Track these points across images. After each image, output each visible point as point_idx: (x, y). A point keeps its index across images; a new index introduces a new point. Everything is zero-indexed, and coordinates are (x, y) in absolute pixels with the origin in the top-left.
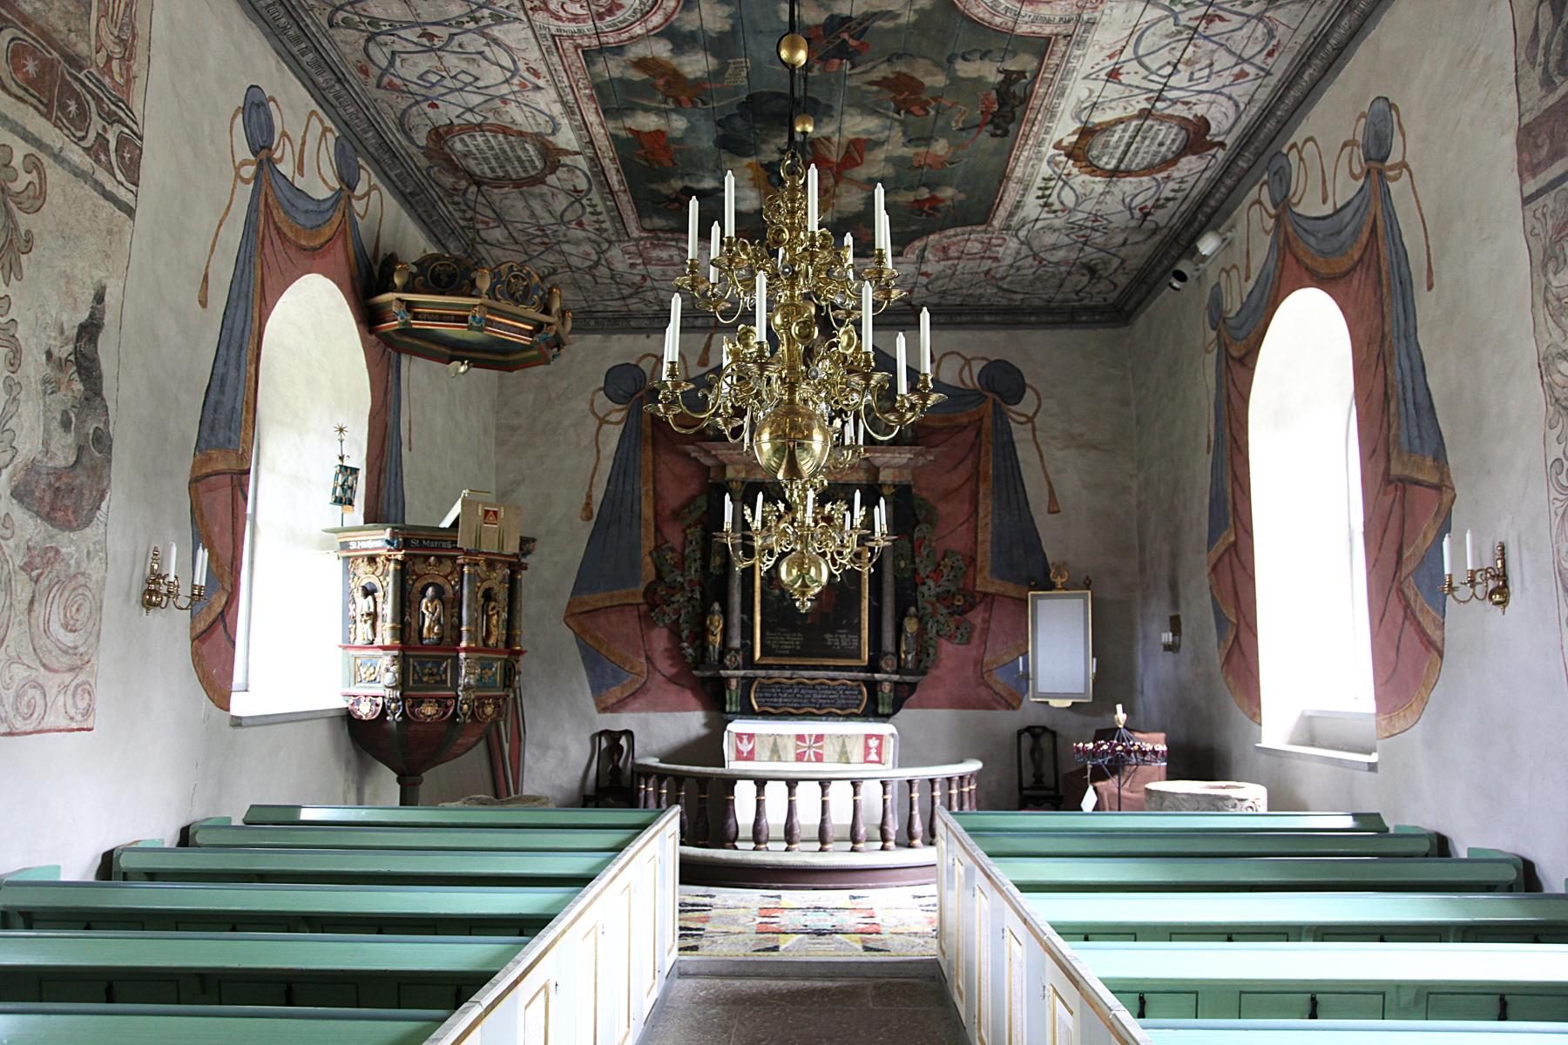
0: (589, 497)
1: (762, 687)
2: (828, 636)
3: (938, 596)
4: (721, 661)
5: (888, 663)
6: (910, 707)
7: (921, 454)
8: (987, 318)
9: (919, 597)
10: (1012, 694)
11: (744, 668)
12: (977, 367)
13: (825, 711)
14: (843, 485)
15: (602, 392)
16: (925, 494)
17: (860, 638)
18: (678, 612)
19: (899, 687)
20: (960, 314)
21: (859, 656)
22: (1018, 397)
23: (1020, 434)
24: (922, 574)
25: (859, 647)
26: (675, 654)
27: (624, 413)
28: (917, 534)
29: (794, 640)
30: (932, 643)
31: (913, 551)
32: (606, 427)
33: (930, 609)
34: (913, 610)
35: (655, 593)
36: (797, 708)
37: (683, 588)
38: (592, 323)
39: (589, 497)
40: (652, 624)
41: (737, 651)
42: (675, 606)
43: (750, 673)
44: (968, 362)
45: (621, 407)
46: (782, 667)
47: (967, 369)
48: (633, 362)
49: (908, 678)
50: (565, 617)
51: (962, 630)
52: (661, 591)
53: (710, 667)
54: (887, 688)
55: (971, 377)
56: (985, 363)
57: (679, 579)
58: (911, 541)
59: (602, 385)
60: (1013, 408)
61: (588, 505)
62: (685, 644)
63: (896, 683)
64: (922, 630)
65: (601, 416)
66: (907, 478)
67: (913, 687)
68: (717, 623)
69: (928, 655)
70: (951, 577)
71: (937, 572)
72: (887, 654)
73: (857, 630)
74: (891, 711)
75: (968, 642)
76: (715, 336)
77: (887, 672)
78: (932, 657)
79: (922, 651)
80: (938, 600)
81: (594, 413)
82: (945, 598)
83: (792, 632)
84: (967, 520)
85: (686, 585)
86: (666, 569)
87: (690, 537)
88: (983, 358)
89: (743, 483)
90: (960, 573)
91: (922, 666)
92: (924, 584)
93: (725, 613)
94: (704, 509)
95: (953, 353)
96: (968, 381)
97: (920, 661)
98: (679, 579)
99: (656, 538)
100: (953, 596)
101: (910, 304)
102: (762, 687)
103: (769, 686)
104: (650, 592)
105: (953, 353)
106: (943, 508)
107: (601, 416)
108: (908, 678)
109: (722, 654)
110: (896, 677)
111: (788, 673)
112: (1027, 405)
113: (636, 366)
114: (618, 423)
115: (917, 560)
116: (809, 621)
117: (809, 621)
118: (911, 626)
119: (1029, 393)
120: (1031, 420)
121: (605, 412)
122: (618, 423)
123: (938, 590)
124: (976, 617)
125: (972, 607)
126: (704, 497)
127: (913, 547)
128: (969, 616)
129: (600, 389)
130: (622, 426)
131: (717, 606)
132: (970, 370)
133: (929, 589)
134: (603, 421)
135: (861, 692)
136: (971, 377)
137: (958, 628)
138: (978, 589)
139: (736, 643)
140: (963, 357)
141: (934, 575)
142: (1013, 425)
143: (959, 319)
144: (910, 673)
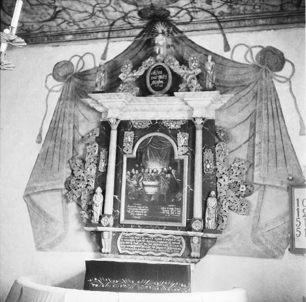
0: (41, 130)
1: (124, 238)
2: (163, 208)
3: (229, 186)
4: (100, 222)
5: (197, 225)
6: (212, 253)
7: (217, 100)
8: (261, 22)
9: (218, 186)
10: (277, 248)
11: (114, 226)
12: (256, 51)
13: (160, 254)
14: (174, 120)
15: (51, 77)
16: (223, 125)
17: (182, 210)
18: (80, 193)
19: (205, 241)
20: (244, 20)
21: (180, 221)
22: (280, 67)
23: (281, 89)
24: (221, 172)
25: (181, 216)
26: (80, 218)
27: (61, 86)
28: (217, 148)
29: (142, 210)
30: (224, 214)
31: (215, 158)
32: (52, 94)
33: (224, 193)
34: (213, 193)
35: (70, 183)
36: (143, 252)
37: (83, 180)
38: (46, 39)
39: (41, 130)
40: (68, 202)
41: (109, 216)
42: (80, 190)
43: (117, 229)
44: (250, 49)
45: (61, 83)
46: (136, 226)
47: (249, 54)
48: (68, 60)
49: (210, 235)
50: (24, 197)
51: (244, 206)
52: (73, 182)
53: (95, 225)
54: (195, 240)
55: (252, 57)
56: (260, 49)
57: (82, 174)
58: (214, 152)
59: (51, 72)
60: (277, 73)
61: (40, 135)
62: (83, 212)
63: (202, 238)
64: (219, 205)
65: (50, 87)
66: (211, 116)
67: (214, 240)
68: (98, 199)
69: (223, 221)
70: (238, 174)
71: (230, 169)
72: (195, 219)
73: (179, 204)
74: (199, 256)
75: (248, 214)
76: (111, 44)
77: (195, 231)
78: (225, 223)
79: (219, 219)
80: (229, 188)
81: (46, 86)
82: (234, 186)
83: (142, 206)
84: (248, 140)
85: (85, 178)
86: (76, 169)
87: (88, 151)
88: (259, 46)
89: (117, 120)
90: (244, 172)
91: (219, 228)
92: (221, 177)
93: (104, 193)
94: (98, 135)
95: (241, 44)
96: (250, 60)
97: (219, 225)
98: (82, 174)
99: (73, 153)
100: (239, 186)
101: (213, 15)
102: (124, 238)
103: (128, 238)
104: (67, 183)
105: (241, 44)
106: (235, 132)
107: (50, 87)
108: (210, 235)
109: (101, 217)
110: (201, 234)
111: (138, 230)
112: (287, 70)
113: (69, 62)
114: (58, 91)
115: (217, 164)
116: (152, 199)
117: (152, 199)
118: (212, 202)
119: (287, 66)
120: (289, 80)
121: (52, 86)
122: (58, 91)
123: (230, 181)
124: (253, 199)
125: (250, 193)
126: (98, 129)
127: (215, 156)
128: (248, 198)
129: (51, 74)
130: (59, 94)
131: (99, 190)
132: (252, 53)
133: (224, 182)
134: (50, 91)
135: (181, 243)
136: (252, 57)
137: (242, 205)
138: (255, 181)
139: (109, 209)
140: (247, 46)
141: (227, 173)
142: (276, 83)
143: (243, 23)
144: (211, 231)
